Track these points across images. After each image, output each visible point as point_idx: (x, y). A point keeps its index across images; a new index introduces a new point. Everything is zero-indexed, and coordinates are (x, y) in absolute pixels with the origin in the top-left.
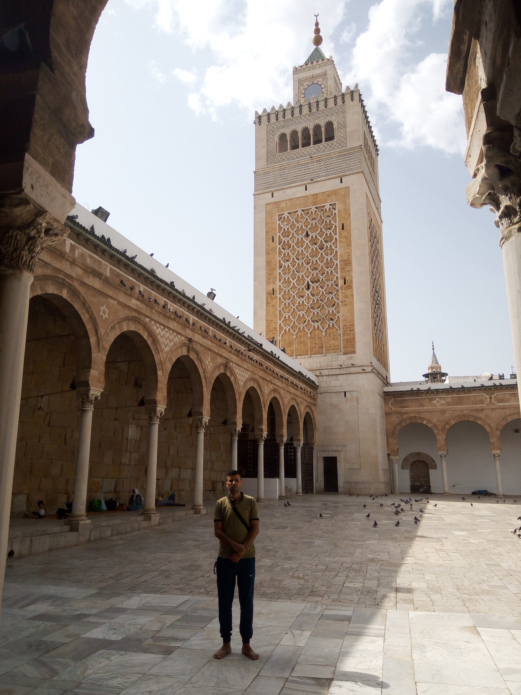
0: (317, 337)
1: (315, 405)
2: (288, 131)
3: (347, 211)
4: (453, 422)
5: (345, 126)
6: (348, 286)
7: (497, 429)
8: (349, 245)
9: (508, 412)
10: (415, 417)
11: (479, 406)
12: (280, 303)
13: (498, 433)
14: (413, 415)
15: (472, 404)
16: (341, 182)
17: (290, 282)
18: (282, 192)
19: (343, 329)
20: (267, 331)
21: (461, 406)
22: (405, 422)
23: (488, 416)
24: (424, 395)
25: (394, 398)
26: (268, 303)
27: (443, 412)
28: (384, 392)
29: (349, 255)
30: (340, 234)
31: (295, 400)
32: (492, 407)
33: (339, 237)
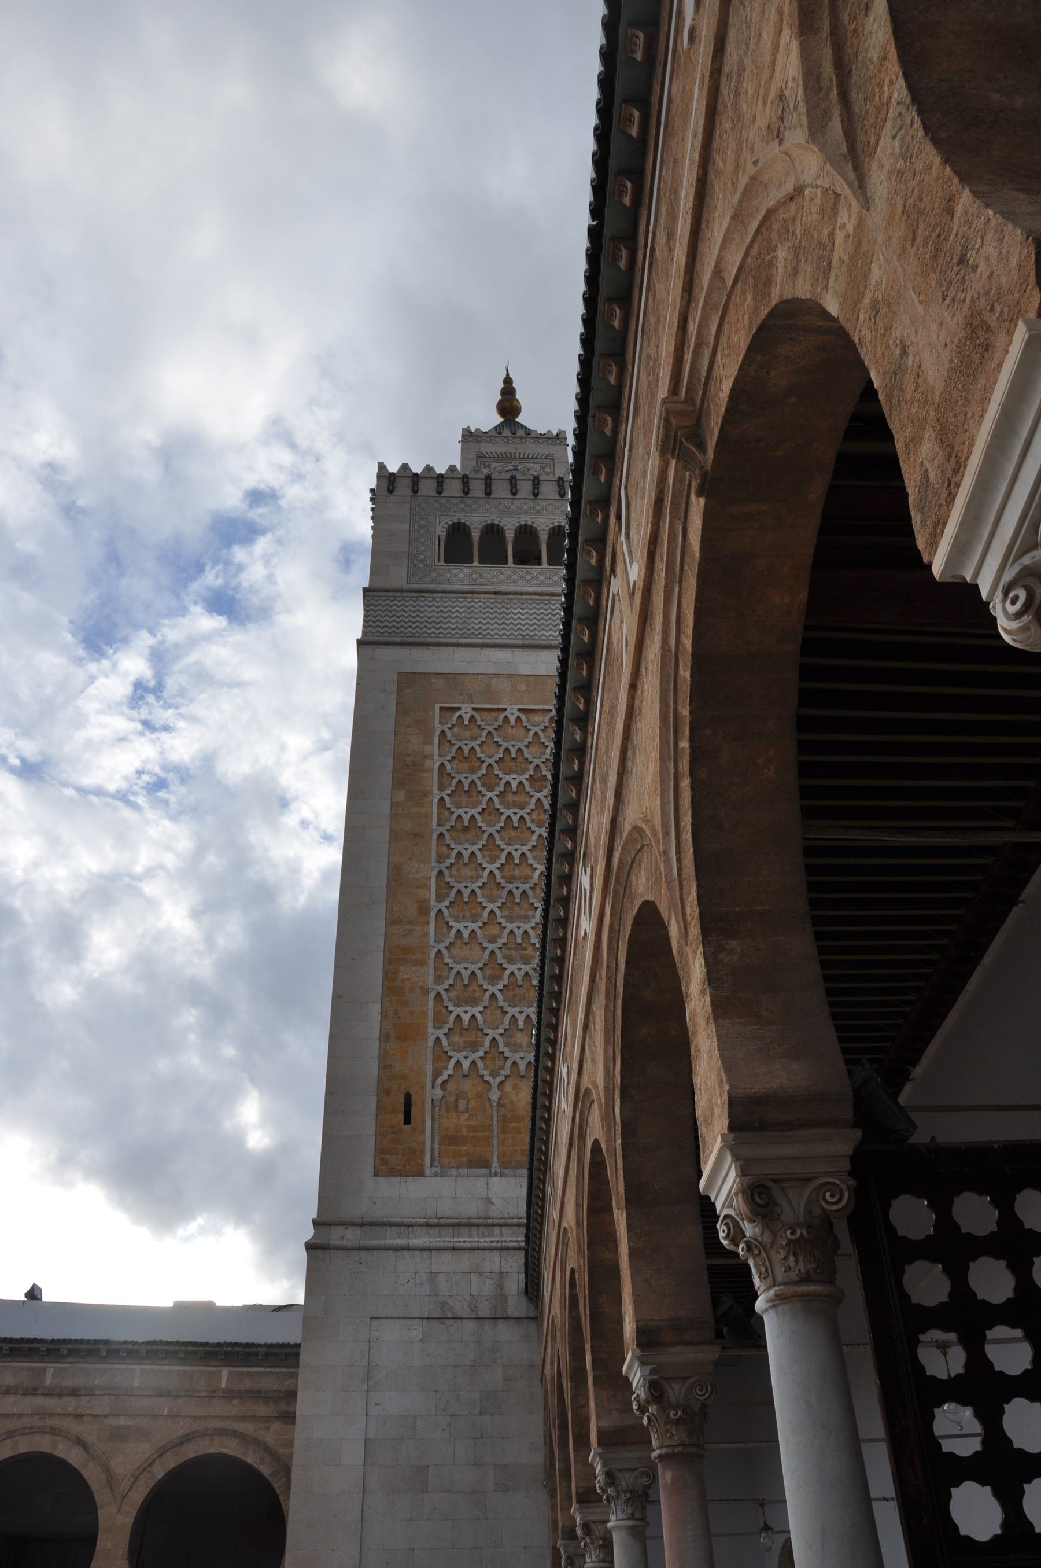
31: (53, 1431)
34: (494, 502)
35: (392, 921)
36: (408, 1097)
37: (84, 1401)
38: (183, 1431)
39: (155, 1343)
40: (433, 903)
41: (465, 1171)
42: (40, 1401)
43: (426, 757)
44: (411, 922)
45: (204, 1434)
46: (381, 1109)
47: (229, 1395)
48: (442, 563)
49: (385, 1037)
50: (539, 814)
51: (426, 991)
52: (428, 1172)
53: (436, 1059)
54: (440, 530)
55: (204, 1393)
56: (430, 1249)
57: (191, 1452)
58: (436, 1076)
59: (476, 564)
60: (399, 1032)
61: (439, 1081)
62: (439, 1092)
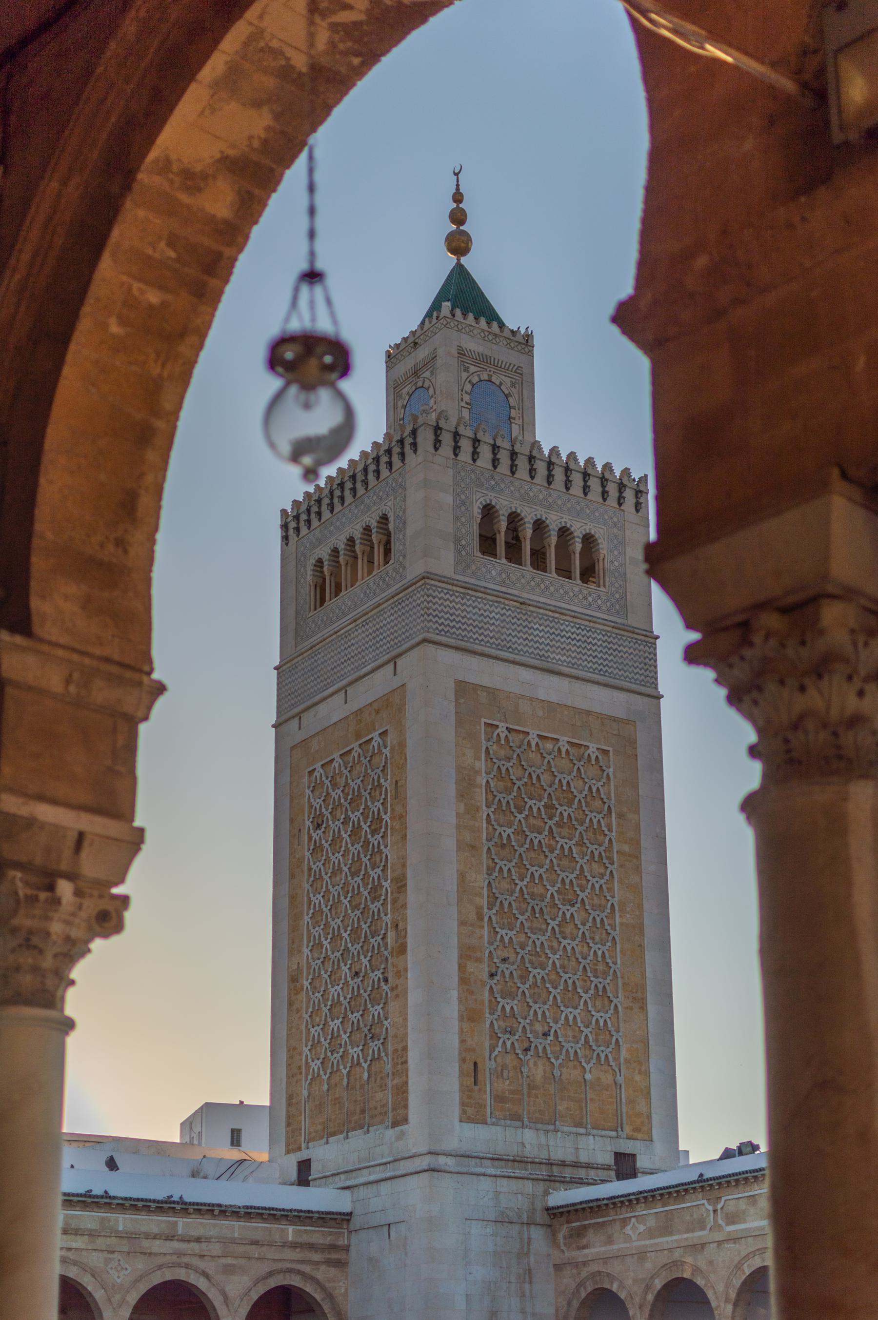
0: (358, 1087)
1: (341, 1264)
2: (324, 552)
3: (402, 745)
4: (658, 1284)
5: (404, 523)
6: (402, 944)
7: (727, 1301)
8: (404, 837)
9: (744, 1248)
10: (599, 1272)
11: (699, 1235)
12: (308, 1001)
13: (730, 1308)
14: (594, 1268)
15: (688, 1231)
16: (395, 674)
17: (321, 945)
18: (312, 712)
19: (393, 1059)
20: (288, 1078)
21: (669, 1239)
22: (585, 1288)
23: (711, 1262)
24: (612, 1212)
25: (568, 1222)
26: (290, 1004)
27: (641, 1255)
28: (548, 1209)
29: (404, 866)
30: (392, 810)
31: (187, 1266)
32: (718, 1236)
33: (391, 818)
34: (517, 483)
35: (462, 923)
36: (475, 1064)
37: (204, 1246)
38: (267, 1270)
39: (251, 1207)
40: (486, 910)
41: (508, 1122)
42: (176, 1245)
43: (478, 772)
44: (472, 925)
45: (280, 1271)
46: (462, 1074)
47: (294, 1246)
48: (479, 554)
49: (461, 1019)
50: (549, 840)
51: (484, 984)
52: (489, 1121)
53: (491, 1038)
54: (477, 512)
55: (279, 1244)
56: (495, 1176)
57: (273, 1283)
58: (491, 1052)
59: (504, 561)
60: (470, 1016)
61: (493, 1055)
62: (493, 1062)
